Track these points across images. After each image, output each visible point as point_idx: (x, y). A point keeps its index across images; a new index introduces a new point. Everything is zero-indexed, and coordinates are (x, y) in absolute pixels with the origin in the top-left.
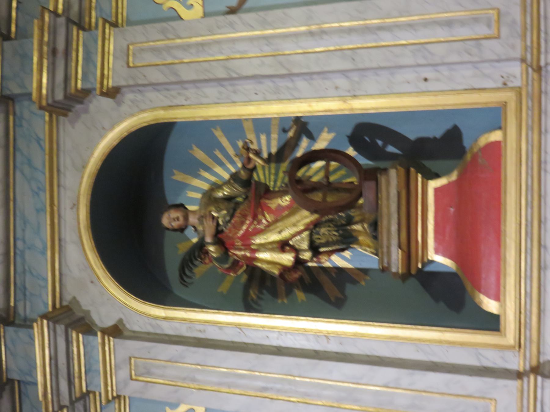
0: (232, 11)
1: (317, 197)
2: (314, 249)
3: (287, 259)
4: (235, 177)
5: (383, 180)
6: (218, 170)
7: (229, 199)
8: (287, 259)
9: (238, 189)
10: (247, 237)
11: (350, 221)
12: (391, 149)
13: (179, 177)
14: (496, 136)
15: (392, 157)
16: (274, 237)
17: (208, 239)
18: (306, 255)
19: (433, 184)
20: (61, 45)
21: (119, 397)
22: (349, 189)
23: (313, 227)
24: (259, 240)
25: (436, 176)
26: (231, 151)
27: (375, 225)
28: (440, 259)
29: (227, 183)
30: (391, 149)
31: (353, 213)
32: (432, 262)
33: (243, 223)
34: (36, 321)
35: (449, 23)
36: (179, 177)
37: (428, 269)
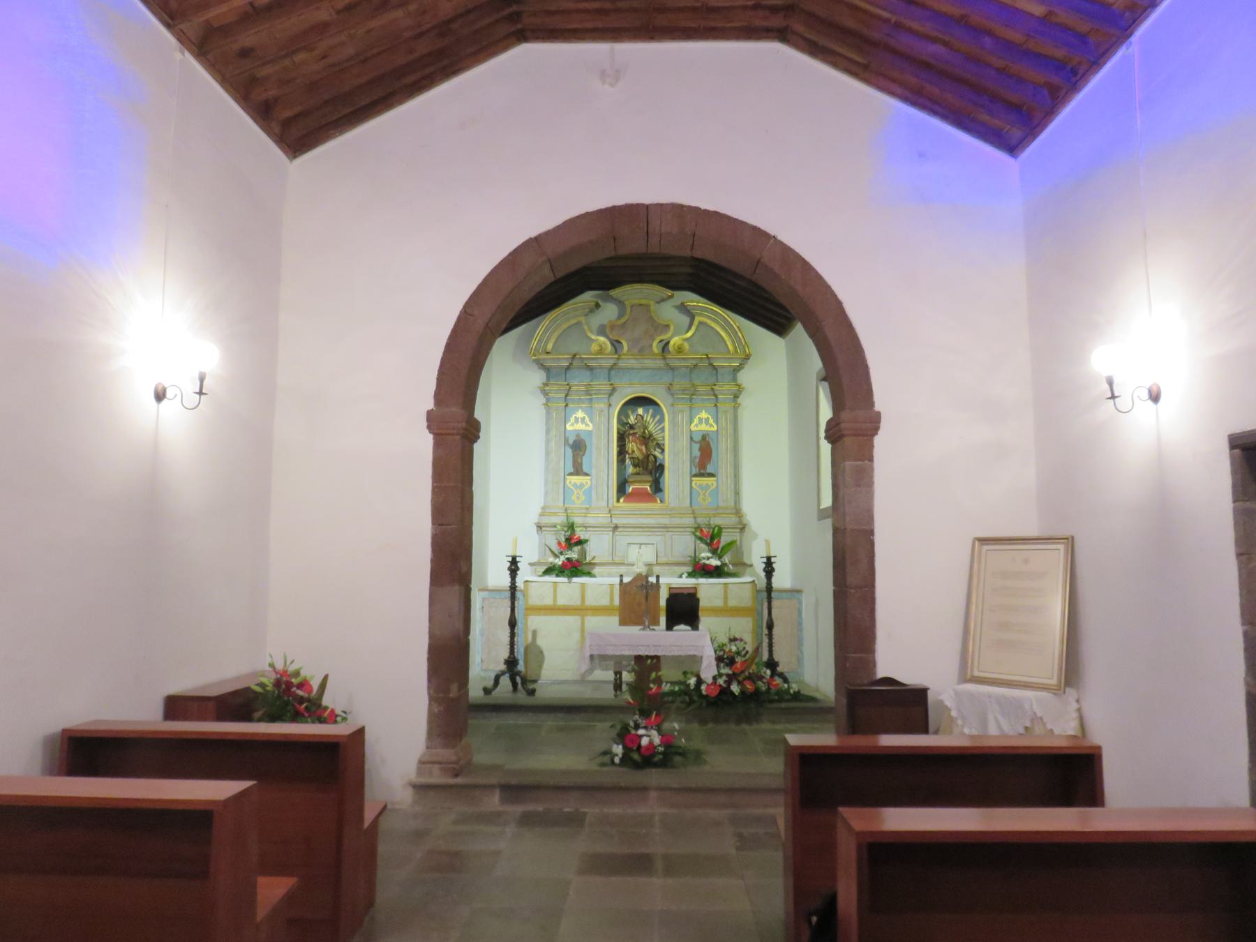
0: (691, 438)
1: (646, 460)
2: (632, 458)
3: (630, 451)
4: (651, 435)
5: (649, 476)
6: (653, 424)
7: (644, 432)
8: (630, 451)
9: (648, 436)
10: (635, 442)
11: (639, 467)
12: (658, 475)
13: (651, 411)
14: (659, 501)
15: (655, 475)
16: (635, 449)
17: (635, 431)
18: (631, 456)
19: (648, 488)
20: (685, 392)
21: (591, 407)
22: (647, 465)
23: (638, 458)
24: (635, 445)
25: (650, 486)
26: (658, 428)
27: (638, 474)
28: (631, 489)
29: (648, 431)
30: (658, 475)
31: (641, 469)
32: (630, 486)
33: (640, 440)
34: (609, 381)
35: (683, 492)
36: (651, 411)
37: (627, 484)
